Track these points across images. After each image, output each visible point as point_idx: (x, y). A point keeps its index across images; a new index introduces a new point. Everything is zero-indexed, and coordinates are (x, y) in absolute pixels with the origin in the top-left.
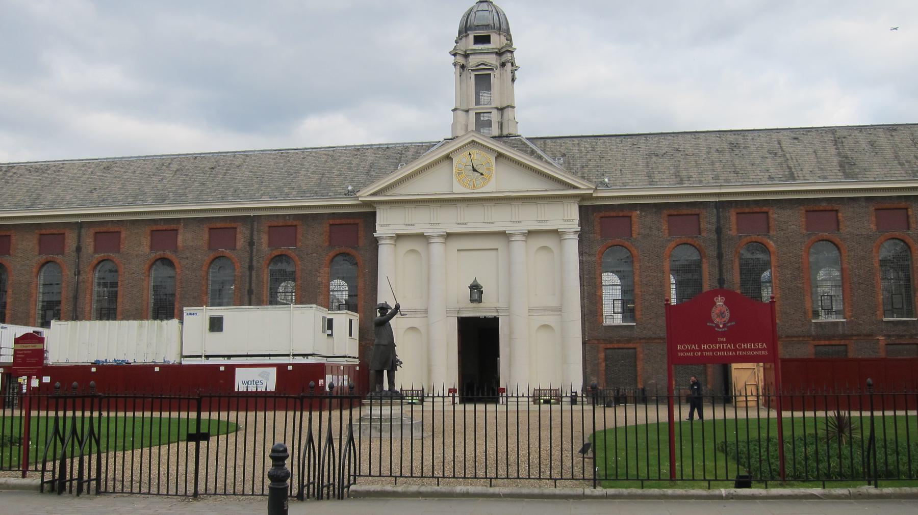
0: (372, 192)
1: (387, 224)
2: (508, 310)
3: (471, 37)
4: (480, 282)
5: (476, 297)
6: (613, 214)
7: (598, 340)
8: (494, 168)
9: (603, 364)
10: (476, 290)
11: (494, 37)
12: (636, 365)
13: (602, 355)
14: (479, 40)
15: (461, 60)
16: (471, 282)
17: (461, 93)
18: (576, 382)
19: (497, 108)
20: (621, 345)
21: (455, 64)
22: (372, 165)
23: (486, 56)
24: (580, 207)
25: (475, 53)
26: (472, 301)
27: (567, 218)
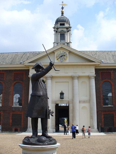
3: (59, 24)
4: (63, 92)
5: (62, 97)
7: (101, 111)
8: (68, 57)
9: (103, 119)
10: (62, 94)
11: (66, 24)
12: (113, 120)
14: (61, 25)
16: (60, 92)
17: (56, 38)
20: (109, 113)
21: (54, 31)
22: (28, 57)
24: (95, 69)
25: (60, 28)
26: (61, 98)
27: (92, 72)
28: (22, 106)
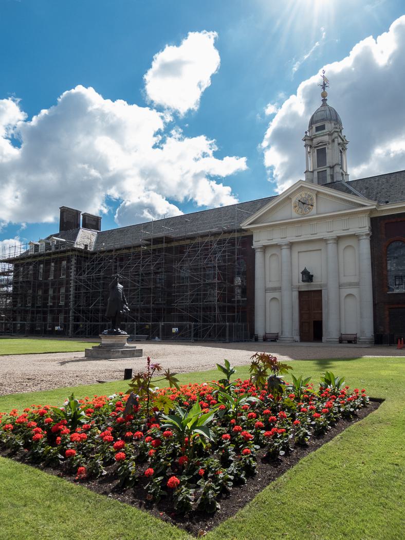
0: (249, 223)
1: (259, 241)
2: (326, 285)
6: (394, 220)
13: (387, 313)
14: (318, 129)
15: (308, 142)
18: (368, 331)
19: (330, 167)
23: (323, 137)
27: (362, 226)
28: (246, 299)
